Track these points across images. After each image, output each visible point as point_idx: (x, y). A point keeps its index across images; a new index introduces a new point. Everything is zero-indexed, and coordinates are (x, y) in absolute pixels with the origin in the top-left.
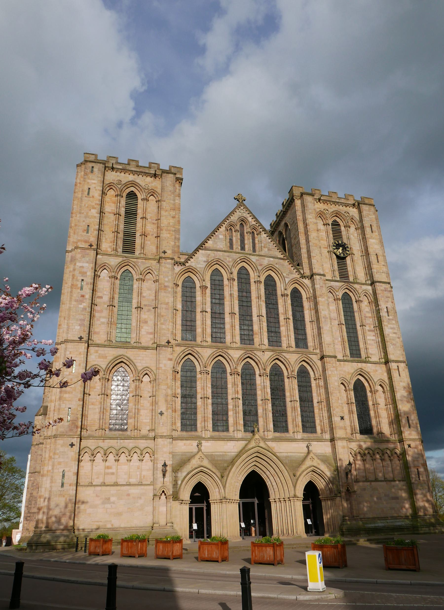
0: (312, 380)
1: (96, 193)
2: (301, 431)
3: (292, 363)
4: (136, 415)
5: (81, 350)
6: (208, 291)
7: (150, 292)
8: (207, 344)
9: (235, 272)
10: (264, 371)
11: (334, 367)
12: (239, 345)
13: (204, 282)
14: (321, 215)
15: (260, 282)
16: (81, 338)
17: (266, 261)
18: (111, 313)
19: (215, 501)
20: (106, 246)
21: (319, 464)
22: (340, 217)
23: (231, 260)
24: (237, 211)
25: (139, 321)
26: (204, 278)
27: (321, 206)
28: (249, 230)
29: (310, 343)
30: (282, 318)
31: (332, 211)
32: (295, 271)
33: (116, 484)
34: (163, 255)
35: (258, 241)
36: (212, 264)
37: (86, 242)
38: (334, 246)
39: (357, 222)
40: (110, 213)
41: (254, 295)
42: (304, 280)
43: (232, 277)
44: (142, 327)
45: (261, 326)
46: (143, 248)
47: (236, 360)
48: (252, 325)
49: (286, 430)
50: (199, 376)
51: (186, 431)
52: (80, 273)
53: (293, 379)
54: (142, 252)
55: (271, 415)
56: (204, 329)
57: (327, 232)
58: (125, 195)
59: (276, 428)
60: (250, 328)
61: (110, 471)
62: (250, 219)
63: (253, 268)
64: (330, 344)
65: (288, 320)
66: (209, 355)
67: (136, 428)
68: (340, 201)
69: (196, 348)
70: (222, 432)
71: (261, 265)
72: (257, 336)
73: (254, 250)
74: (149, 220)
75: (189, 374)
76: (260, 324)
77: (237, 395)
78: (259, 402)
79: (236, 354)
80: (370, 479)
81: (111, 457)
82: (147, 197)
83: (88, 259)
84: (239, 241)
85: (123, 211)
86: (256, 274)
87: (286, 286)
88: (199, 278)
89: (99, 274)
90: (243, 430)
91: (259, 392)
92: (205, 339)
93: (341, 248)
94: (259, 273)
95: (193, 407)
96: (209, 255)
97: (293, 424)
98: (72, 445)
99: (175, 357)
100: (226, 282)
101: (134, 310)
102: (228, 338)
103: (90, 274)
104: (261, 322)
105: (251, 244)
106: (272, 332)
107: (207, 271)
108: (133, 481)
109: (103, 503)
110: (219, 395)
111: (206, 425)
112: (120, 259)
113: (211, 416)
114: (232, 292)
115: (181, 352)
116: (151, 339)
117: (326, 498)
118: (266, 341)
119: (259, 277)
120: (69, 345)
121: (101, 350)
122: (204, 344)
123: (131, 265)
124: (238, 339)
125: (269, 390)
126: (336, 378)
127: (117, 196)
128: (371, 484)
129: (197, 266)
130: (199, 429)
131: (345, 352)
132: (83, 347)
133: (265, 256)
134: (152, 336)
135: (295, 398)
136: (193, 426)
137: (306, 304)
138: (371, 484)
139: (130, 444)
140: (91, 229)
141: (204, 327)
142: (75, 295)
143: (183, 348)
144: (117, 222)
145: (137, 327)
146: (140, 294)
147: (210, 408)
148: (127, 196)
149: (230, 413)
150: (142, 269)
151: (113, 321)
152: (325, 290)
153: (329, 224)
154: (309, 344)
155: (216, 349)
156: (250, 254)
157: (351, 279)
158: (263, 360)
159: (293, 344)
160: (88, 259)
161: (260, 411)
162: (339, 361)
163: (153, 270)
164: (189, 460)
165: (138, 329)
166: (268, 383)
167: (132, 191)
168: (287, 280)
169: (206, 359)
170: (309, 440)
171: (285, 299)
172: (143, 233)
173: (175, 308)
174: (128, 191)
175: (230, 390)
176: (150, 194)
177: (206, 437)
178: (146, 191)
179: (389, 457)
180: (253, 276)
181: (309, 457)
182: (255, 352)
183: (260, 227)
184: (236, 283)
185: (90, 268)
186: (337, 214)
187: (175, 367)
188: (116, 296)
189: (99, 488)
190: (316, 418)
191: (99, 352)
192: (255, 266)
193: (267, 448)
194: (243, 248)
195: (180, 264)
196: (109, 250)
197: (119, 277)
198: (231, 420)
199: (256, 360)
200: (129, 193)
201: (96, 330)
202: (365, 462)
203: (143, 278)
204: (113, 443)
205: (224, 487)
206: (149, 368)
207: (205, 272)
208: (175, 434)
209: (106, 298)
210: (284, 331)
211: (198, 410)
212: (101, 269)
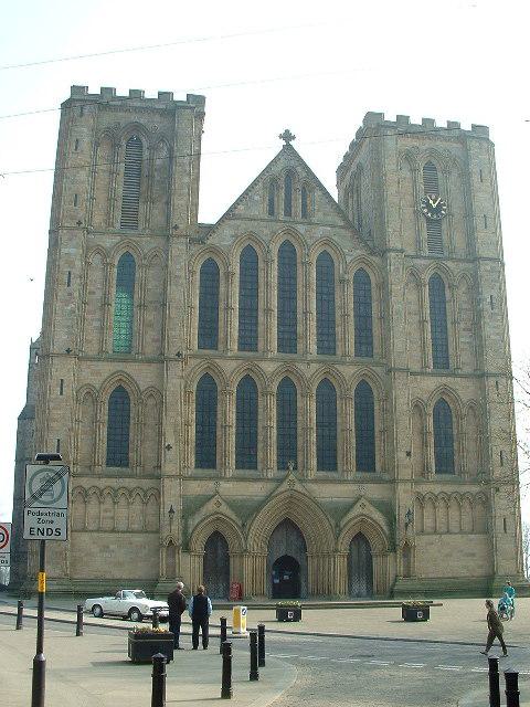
9: (275, 249)
14: (408, 157)
17: (320, 232)
29: (377, 350)
30: (338, 313)
33: (113, 531)
46: (147, 221)
49: (334, 467)
58: (124, 143)
59: (321, 466)
62: (299, 169)
73: (304, 215)
78: (299, 430)
100: (261, 265)
102: (261, 345)
108: (136, 527)
116: (158, 348)
118: (313, 348)
120: (56, 361)
137: (375, 294)
139: (130, 483)
140: (80, 199)
149: (260, 446)
152: (403, 275)
157: (446, 254)
160: (74, 242)
164: (202, 505)
166: (314, 406)
181: (358, 504)
184: (275, 265)
189: (95, 534)
193: (304, 491)
204: (113, 482)
208: (185, 472)
209: (99, 294)
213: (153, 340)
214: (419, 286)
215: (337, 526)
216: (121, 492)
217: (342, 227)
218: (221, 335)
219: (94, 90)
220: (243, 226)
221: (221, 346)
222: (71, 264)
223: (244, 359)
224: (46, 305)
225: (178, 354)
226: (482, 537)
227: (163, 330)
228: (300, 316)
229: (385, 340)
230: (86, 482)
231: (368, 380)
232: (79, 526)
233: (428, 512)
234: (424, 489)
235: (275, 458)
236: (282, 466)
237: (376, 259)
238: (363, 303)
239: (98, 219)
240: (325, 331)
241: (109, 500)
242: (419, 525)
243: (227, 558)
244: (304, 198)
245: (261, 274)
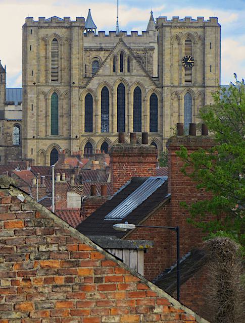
1: (34, 49)
17: (134, 79)
27: (176, 31)
37: (32, 81)
38: (183, 60)
42: (158, 89)
52: (31, 101)
62: (126, 51)
68: (192, 25)
71: (131, 82)
73: (129, 71)
93: (188, 61)
100: (110, 95)
121: (44, 141)
133: (134, 76)
134: (69, 131)
142: (29, 114)
154: (158, 130)
156: (125, 76)
191: (43, 142)
201: (41, 130)
209: (44, 112)
213: (67, 130)
214: (179, 100)
217: (145, 76)
221: (94, 131)
222: (32, 101)
223: (103, 136)
227: (70, 125)
228: (126, 117)
229: (162, 126)
237: (160, 90)
239: (42, 79)
245: (110, 99)
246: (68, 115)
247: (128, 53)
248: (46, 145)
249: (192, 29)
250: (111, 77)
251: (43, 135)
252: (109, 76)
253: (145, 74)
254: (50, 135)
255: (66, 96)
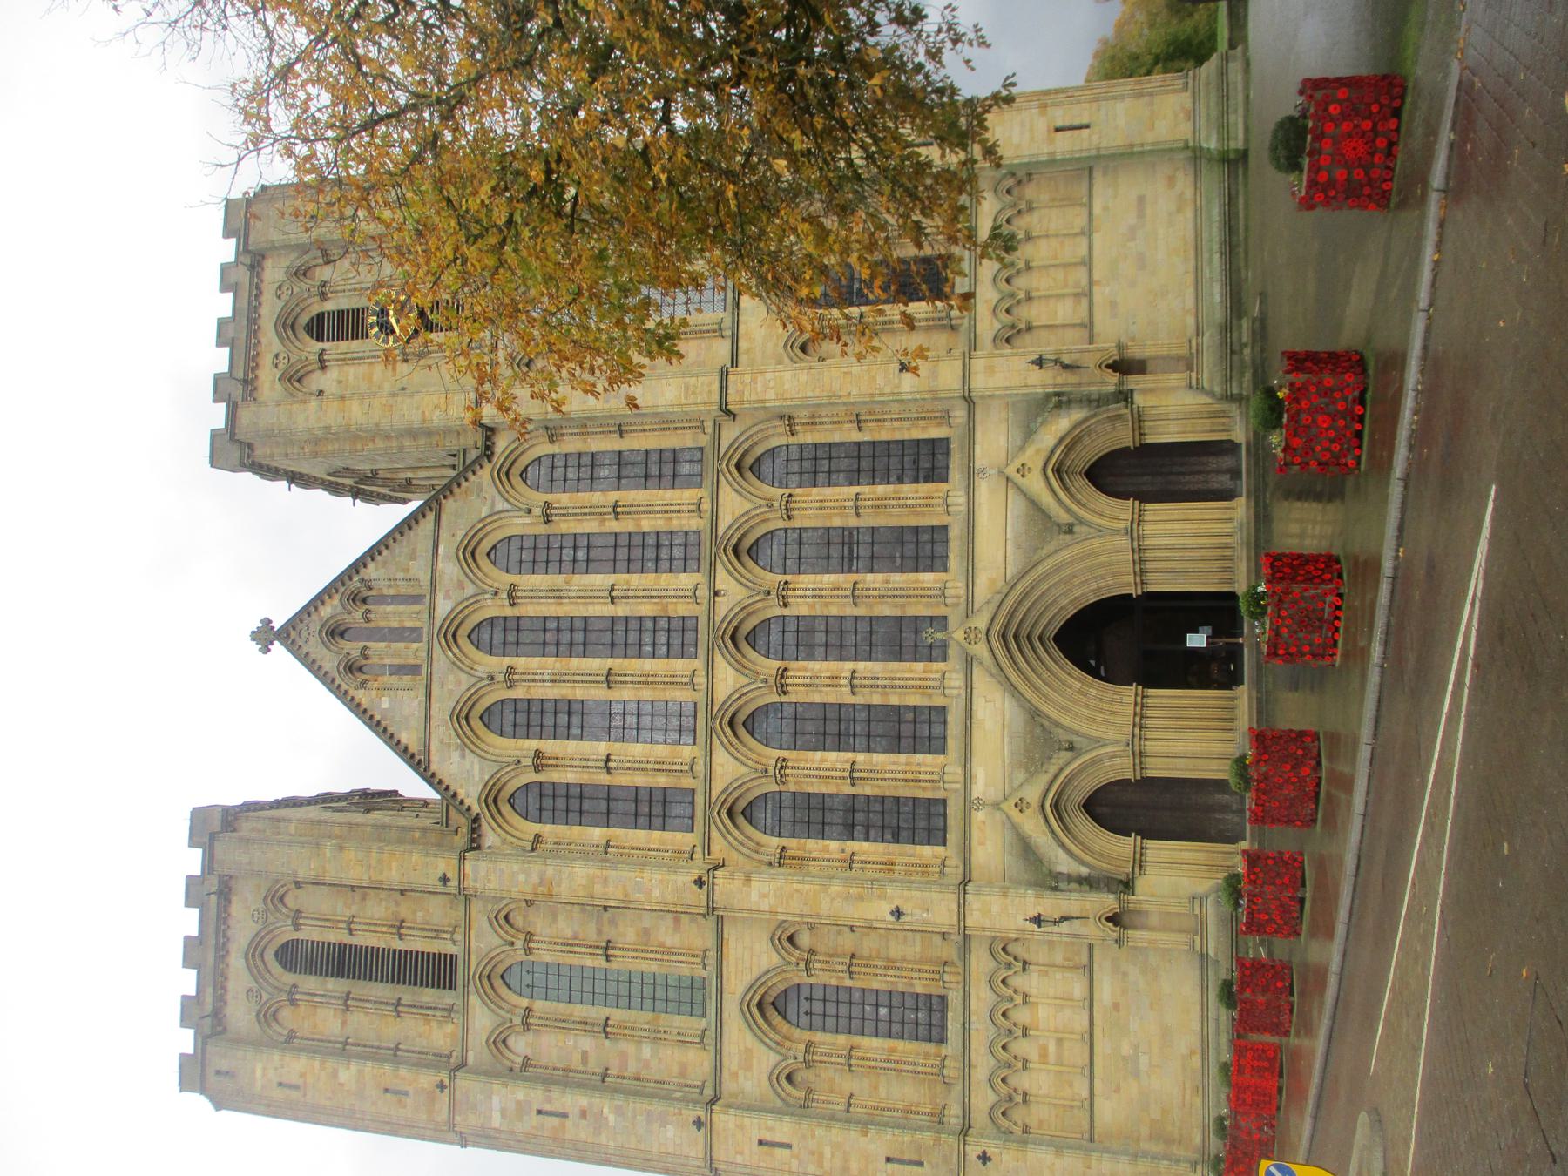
0: (792, 440)
2: (943, 486)
3: (748, 506)
4: (904, 974)
5: (731, 1126)
6: (550, 746)
7: (561, 918)
8: (700, 762)
10: (774, 594)
11: (754, 380)
12: (698, 664)
13: (522, 760)
14: (294, 378)
15: (513, 588)
16: (698, 1123)
17: (449, 569)
18: (626, 1031)
19: (1138, 768)
20: (440, 1036)
21: (1038, 451)
22: (294, 314)
23: (451, 678)
24: (305, 650)
25: (644, 955)
26: (511, 760)
27: (268, 377)
28: (358, 615)
30: (614, 526)
31: (276, 340)
32: (472, 478)
33: (1089, 1038)
34: (454, 883)
35: (390, 586)
36: (469, 733)
39: (306, 257)
40: (344, 1023)
41: (550, 609)
43: (501, 678)
44: (662, 945)
45: (641, 594)
46: (437, 933)
47: (744, 680)
48: (641, 618)
50: (792, 787)
51: (945, 830)
53: (792, 505)
54: (448, 936)
55: (898, 579)
56: (657, 767)
57: (344, 360)
58: (289, 978)
60: (649, 625)
61: (1052, 1048)
62: (326, 611)
63: (471, 609)
64: (687, 387)
65: (619, 510)
66: (731, 759)
67: (937, 976)
69: (714, 794)
70: (949, 726)
71: (461, 586)
72: (670, 608)
73: (415, 599)
74: (354, 910)
75: (787, 814)
76: (636, 597)
77: (842, 682)
78: (860, 611)
79: (727, 679)
80: (1084, 282)
81: (1021, 1047)
82: (288, 916)
83: (481, 1097)
84: (394, 645)
85: (335, 985)
86: (489, 602)
87: (520, 509)
88: (512, 774)
89: (519, 1060)
90: (941, 665)
91: (834, 611)
92: (687, 768)
94: (485, 592)
95: (878, 807)
96: (442, 741)
97: (923, 514)
98: (984, 1158)
99: (741, 857)
100: (519, 693)
101: (614, 965)
103: (520, 1092)
104: (630, 593)
105: (401, 608)
106: (657, 559)
107: (491, 750)
108: (1078, 989)
109: (1136, 1074)
110: (843, 727)
111: (928, 777)
112: (474, 999)
113: (903, 758)
114: (547, 677)
115: (725, 838)
116: (692, 921)
117: (1137, 433)
118: (685, 580)
119: (496, 593)
120: (720, 1154)
121: (731, 1062)
122: (699, 768)
123: (489, 968)
124: (680, 666)
125: (828, 579)
126: (787, 375)
127: (293, 1002)
128: (1098, 283)
129: (477, 778)
130: (940, 795)
131: (708, 331)
132: (723, 1117)
135: (847, 504)
136: (932, 809)
137: (571, 445)
138: (1098, 283)
139: (982, 998)
141: (650, 766)
143: (715, 834)
144: (368, 1005)
145: (662, 960)
146: (567, 945)
147: (880, 758)
148: (290, 970)
149: (894, 700)
150: (498, 941)
151: (648, 1023)
153: (322, 352)
154: (690, 444)
155: (714, 736)
156: (432, 616)
158: (740, 597)
159: (688, 495)
161: (886, 610)
162: (735, 361)
163: (497, 908)
165: (666, 957)
166: (807, 581)
167: (276, 954)
168: (501, 505)
169: (744, 770)
170: (971, 474)
171: (557, 515)
172: (394, 930)
173: (602, 849)
174: (277, 969)
175: (831, 696)
176: (280, 906)
177: (962, 779)
178: (271, 919)
179: (1019, 212)
180: (496, 608)
181: (1017, 477)
182: (718, 619)
183: (346, 579)
184: (521, 663)
185: (504, 1090)
186: (287, 325)
187: (766, 858)
188: (579, 1011)
189: (1098, 1084)
190: (906, 436)
191: (734, 1067)
192: (466, 604)
193: (992, 608)
194: (412, 634)
195: (474, 830)
196: (449, 1028)
197: (525, 1002)
198: (914, 700)
199: (741, 616)
200: (280, 964)
201: (676, 1069)
202: (1034, 294)
203: (522, 937)
205: (1099, 742)
206: (774, 933)
207: (493, 758)
208: (954, 870)
209: (586, 1043)
210: (653, 522)
211: (887, 794)
212: (506, 1052)
215: (1070, 530)
216: (1000, 1019)
217: (438, 518)
218: (662, 781)
219: (185, 1040)
220: (443, 731)
221: (687, 782)
224: (607, 1162)
225: (700, 882)
226: (1098, 175)
228: (621, 610)
230: (983, 1099)
231: (749, 460)
232: (1083, 1116)
233: (1033, 313)
234: (987, 325)
235: (920, 666)
236: (936, 652)
237: (502, 444)
238: (588, 470)
239: (440, 1036)
240: (650, 553)
241: (1021, 1047)
242: (1070, 334)
243: (1148, 783)
244: (383, 599)
245: (538, 692)
246: (606, 915)
247: (336, 600)
248: (748, 1051)
249: (265, 310)
250: (436, 691)
251: (698, 1063)
252: (429, 695)
253: (431, 516)
254: (703, 1023)
255: (518, 920)
